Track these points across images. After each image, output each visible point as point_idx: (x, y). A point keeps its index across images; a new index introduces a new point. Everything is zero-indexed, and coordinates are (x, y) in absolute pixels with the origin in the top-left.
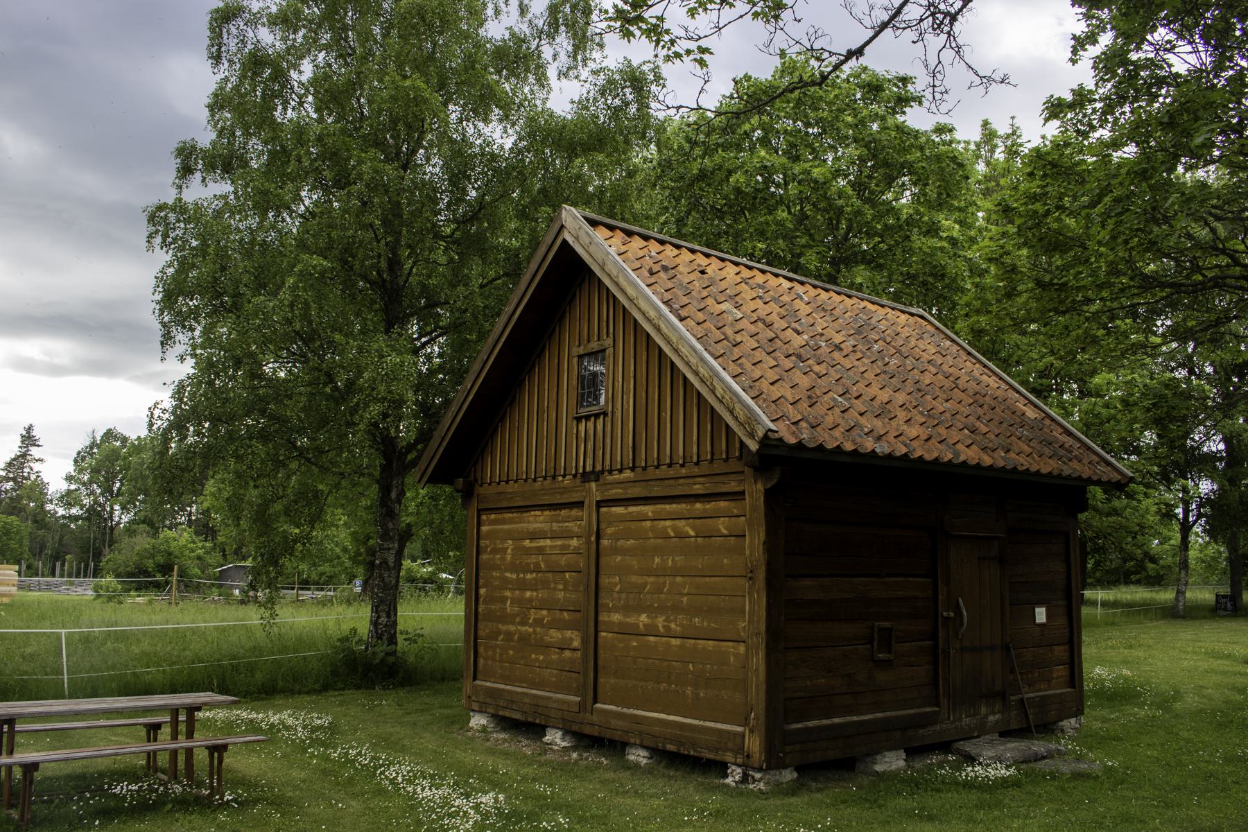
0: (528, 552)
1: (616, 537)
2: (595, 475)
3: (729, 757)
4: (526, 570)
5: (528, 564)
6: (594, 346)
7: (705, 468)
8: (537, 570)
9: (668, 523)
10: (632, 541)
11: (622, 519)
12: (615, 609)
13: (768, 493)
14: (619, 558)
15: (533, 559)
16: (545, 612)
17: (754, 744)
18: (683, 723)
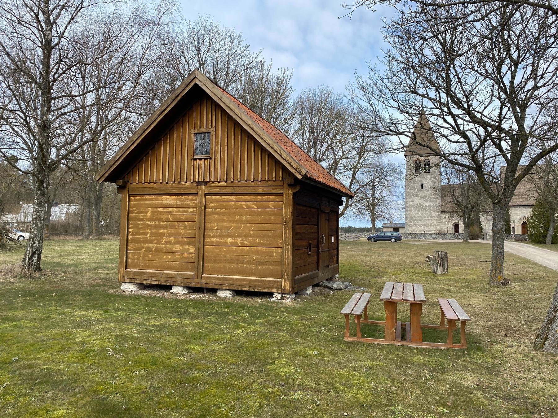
0: (162, 213)
1: (215, 208)
2: (205, 183)
3: (274, 290)
4: (161, 220)
5: (162, 218)
6: (203, 130)
7: (264, 183)
8: (167, 220)
9: (243, 203)
10: (224, 210)
11: (217, 201)
12: (214, 236)
13: (294, 194)
14: (217, 216)
15: (165, 216)
16: (172, 238)
17: (286, 285)
18: (251, 279)
